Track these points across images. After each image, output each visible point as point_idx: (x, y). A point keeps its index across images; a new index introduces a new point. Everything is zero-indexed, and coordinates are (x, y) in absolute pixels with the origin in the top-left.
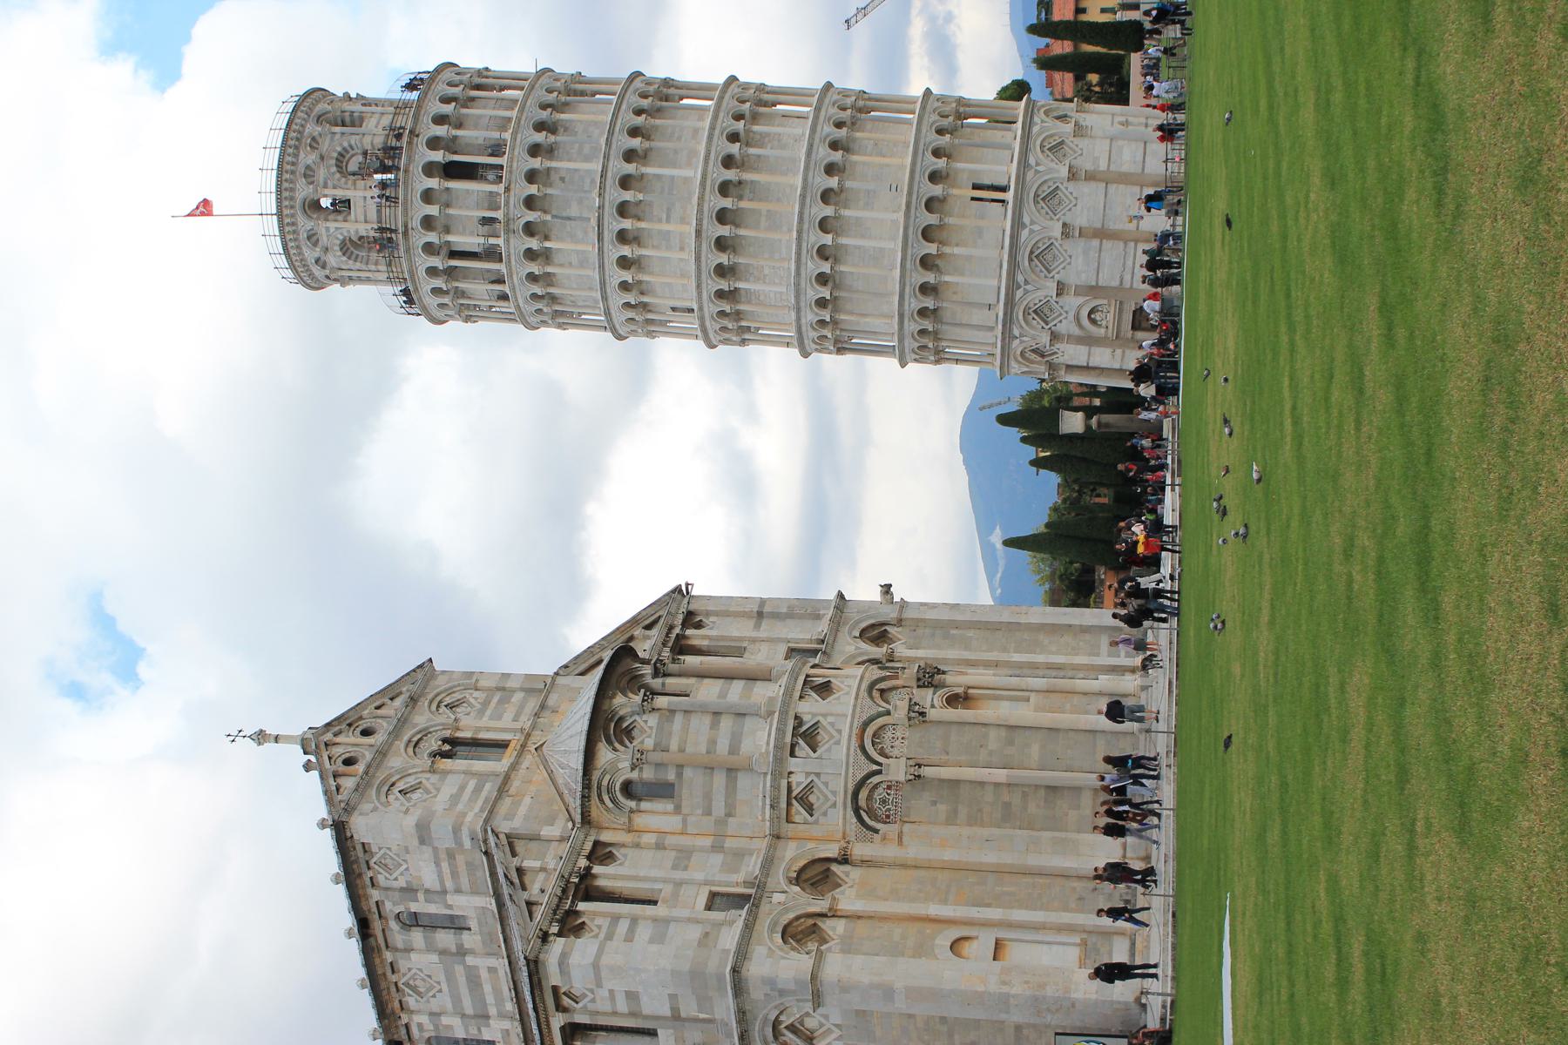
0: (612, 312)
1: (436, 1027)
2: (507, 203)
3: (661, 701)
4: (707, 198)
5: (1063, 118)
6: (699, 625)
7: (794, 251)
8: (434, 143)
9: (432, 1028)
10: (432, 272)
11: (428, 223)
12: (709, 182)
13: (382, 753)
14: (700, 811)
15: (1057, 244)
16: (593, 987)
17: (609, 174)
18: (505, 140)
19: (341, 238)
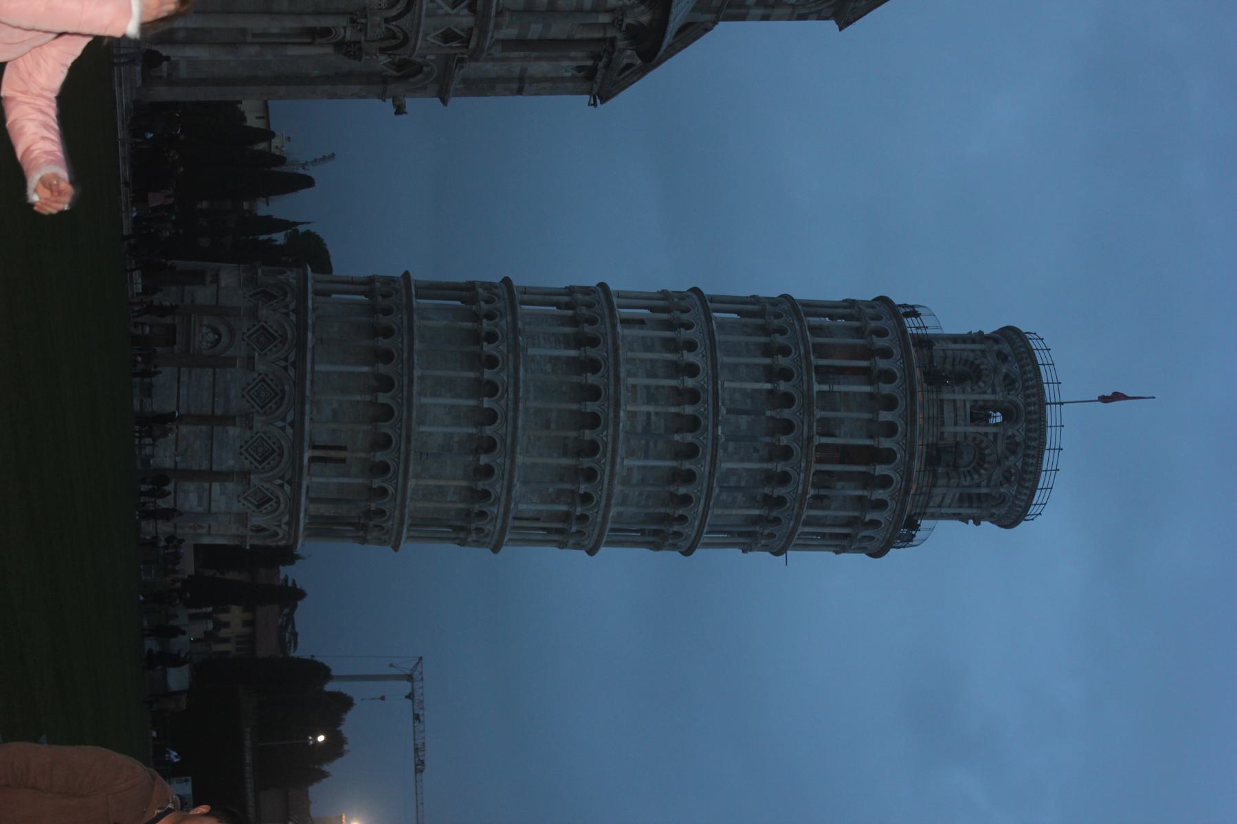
0: (703, 318)
2: (810, 427)
3: (604, 18)
4: (610, 439)
5: (259, 530)
6: (580, 69)
7: (521, 390)
8: (885, 482)
10: (886, 353)
12: (609, 455)
15: (259, 409)
17: (708, 458)
18: (814, 486)
19: (981, 384)
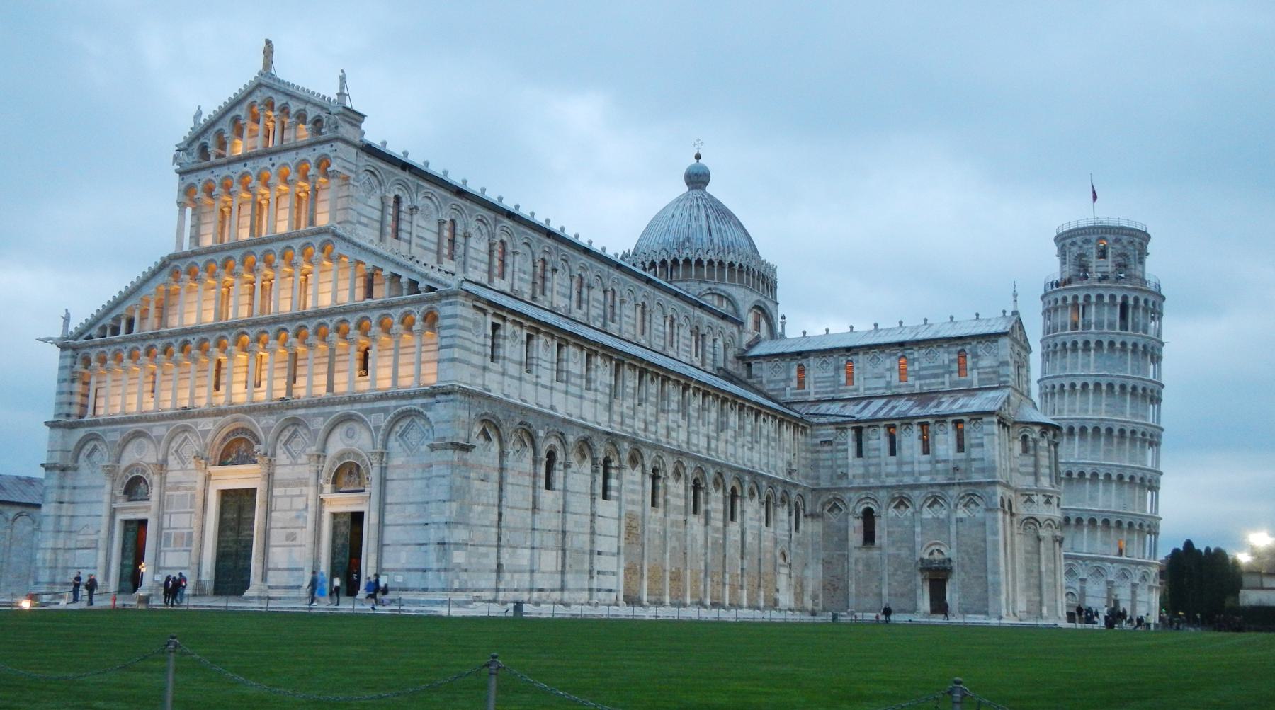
1: (914, 359)
2: (1113, 333)
3: (1052, 448)
5: (1154, 581)
8: (1136, 300)
9: (912, 357)
10: (1076, 297)
11: (1100, 297)
13: (1018, 343)
14: (1020, 462)
16: (984, 432)
18: (1138, 331)
